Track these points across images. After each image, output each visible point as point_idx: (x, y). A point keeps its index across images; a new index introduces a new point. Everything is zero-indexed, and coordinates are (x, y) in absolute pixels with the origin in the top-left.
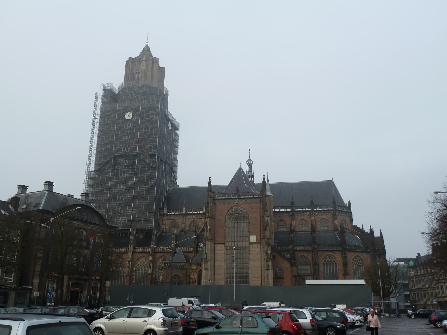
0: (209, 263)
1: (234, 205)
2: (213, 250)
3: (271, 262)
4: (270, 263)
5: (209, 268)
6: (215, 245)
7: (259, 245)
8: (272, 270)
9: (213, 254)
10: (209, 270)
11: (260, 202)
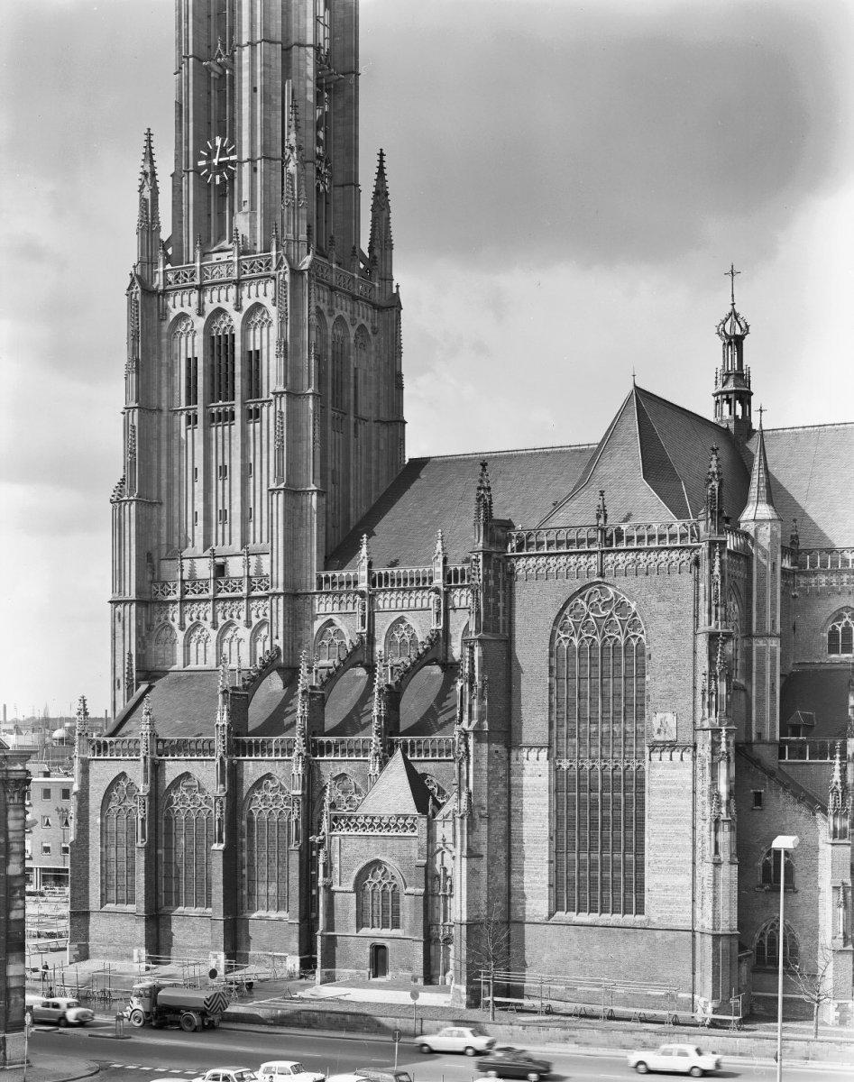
0: (484, 828)
1: (588, 581)
2: (502, 773)
3: (731, 829)
4: (725, 836)
5: (484, 850)
6: (509, 752)
7: (688, 756)
8: (731, 863)
9: (501, 788)
10: (485, 858)
11: (697, 563)
